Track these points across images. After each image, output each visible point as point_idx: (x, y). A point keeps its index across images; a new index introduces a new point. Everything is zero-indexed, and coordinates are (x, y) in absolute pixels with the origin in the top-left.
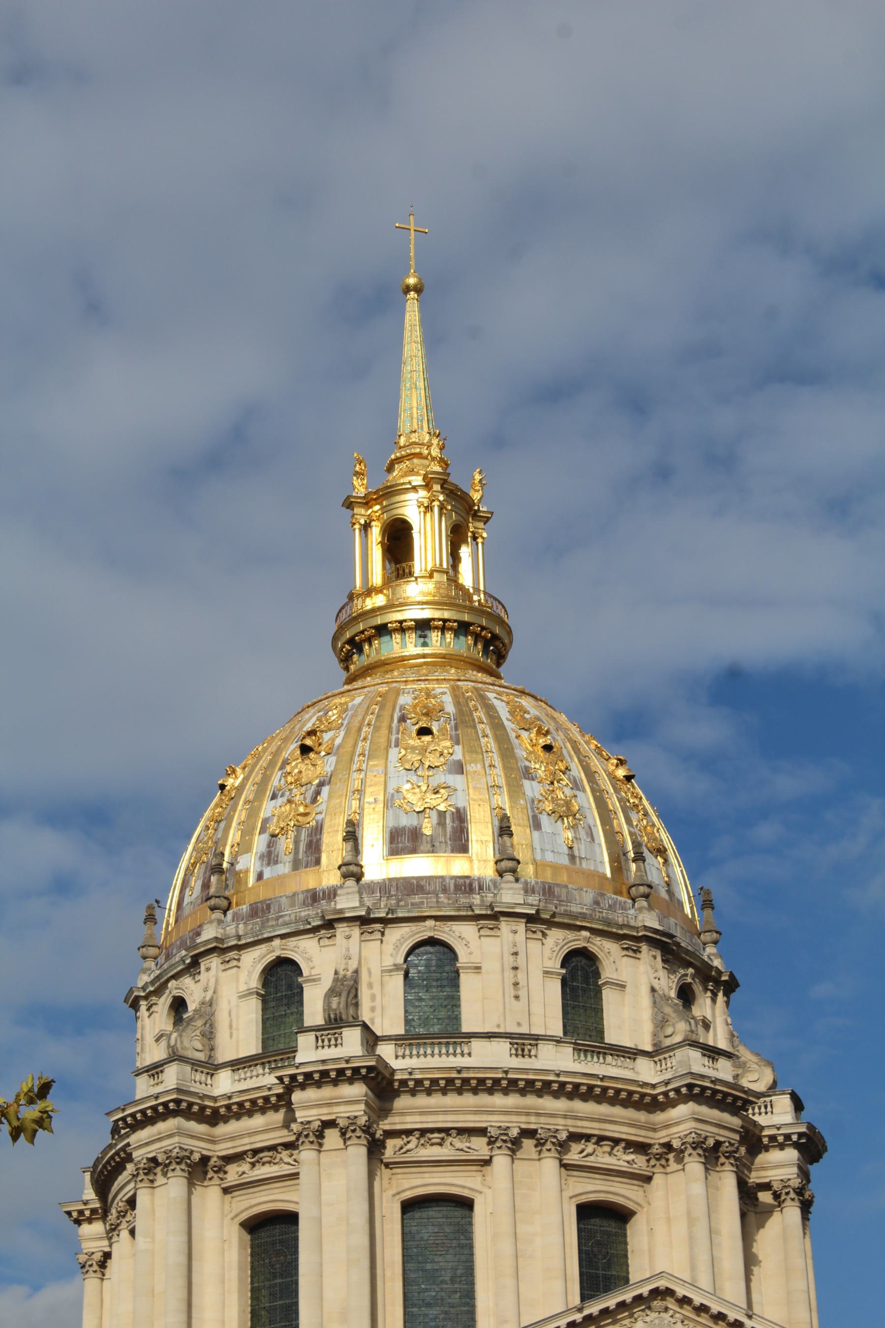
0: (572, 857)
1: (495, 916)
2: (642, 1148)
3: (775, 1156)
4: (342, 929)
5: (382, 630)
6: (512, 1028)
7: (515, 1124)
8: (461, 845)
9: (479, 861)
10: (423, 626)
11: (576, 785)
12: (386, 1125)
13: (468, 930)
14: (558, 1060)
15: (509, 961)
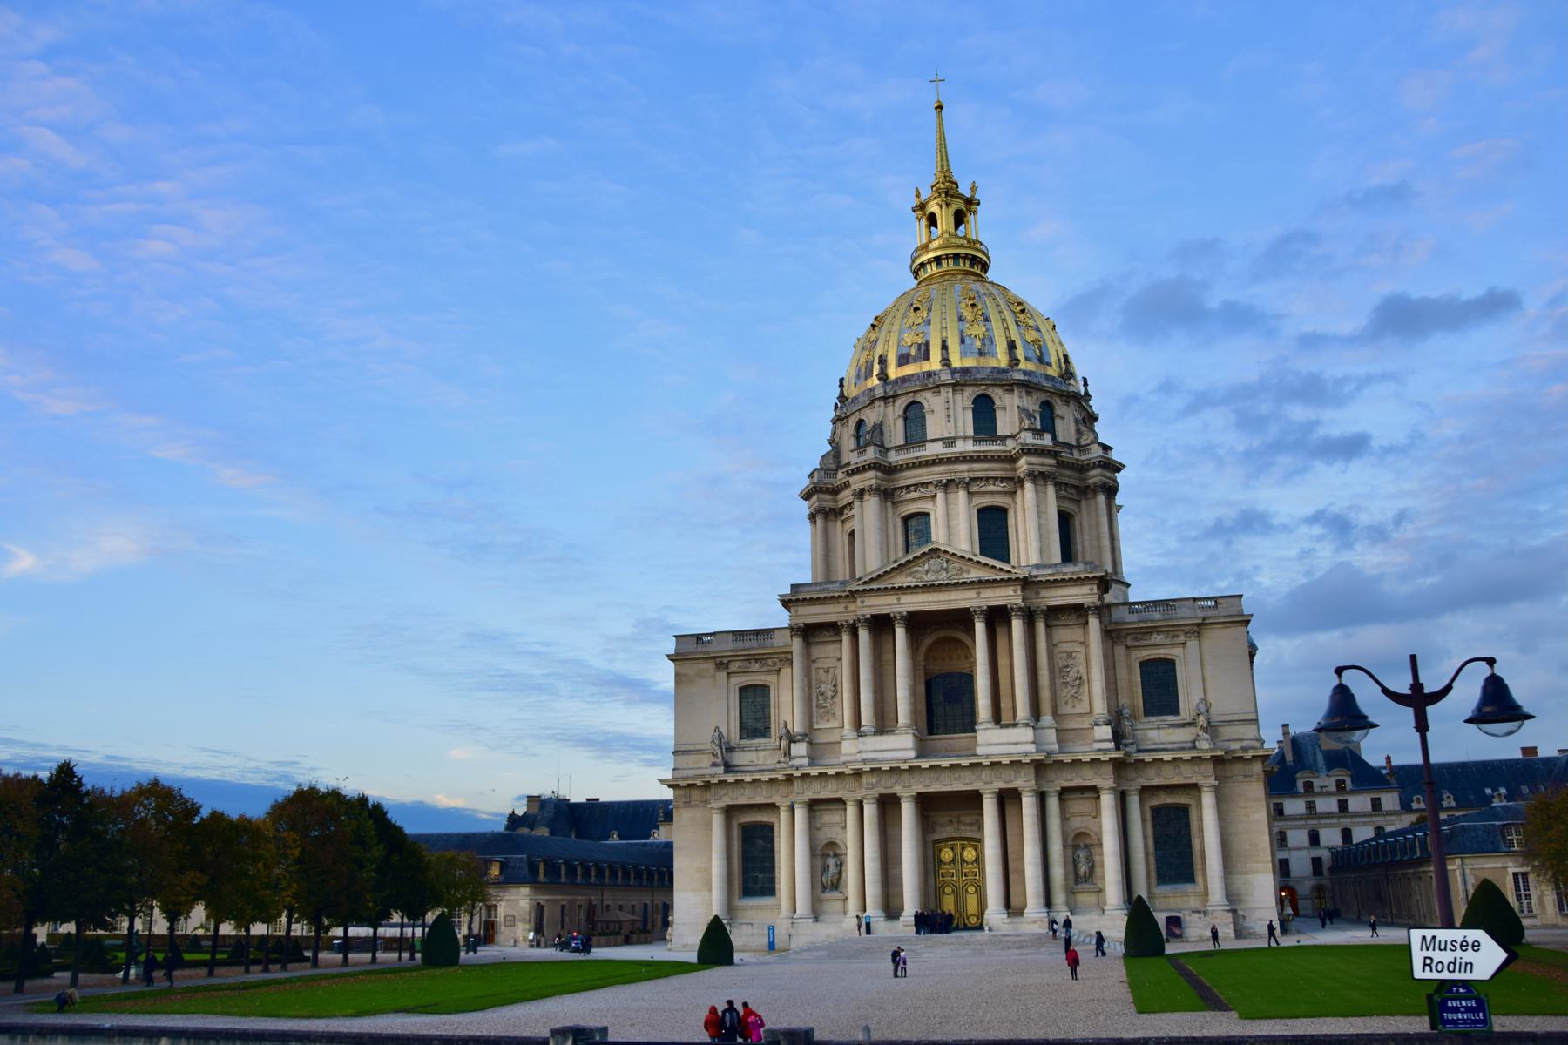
0: (981, 353)
1: (938, 386)
2: (1011, 479)
3: (1093, 473)
4: (877, 403)
5: (922, 265)
6: (946, 435)
7: (944, 478)
8: (927, 357)
9: (934, 364)
10: (938, 260)
11: (987, 320)
12: (892, 485)
13: (928, 395)
14: (965, 447)
15: (944, 405)
